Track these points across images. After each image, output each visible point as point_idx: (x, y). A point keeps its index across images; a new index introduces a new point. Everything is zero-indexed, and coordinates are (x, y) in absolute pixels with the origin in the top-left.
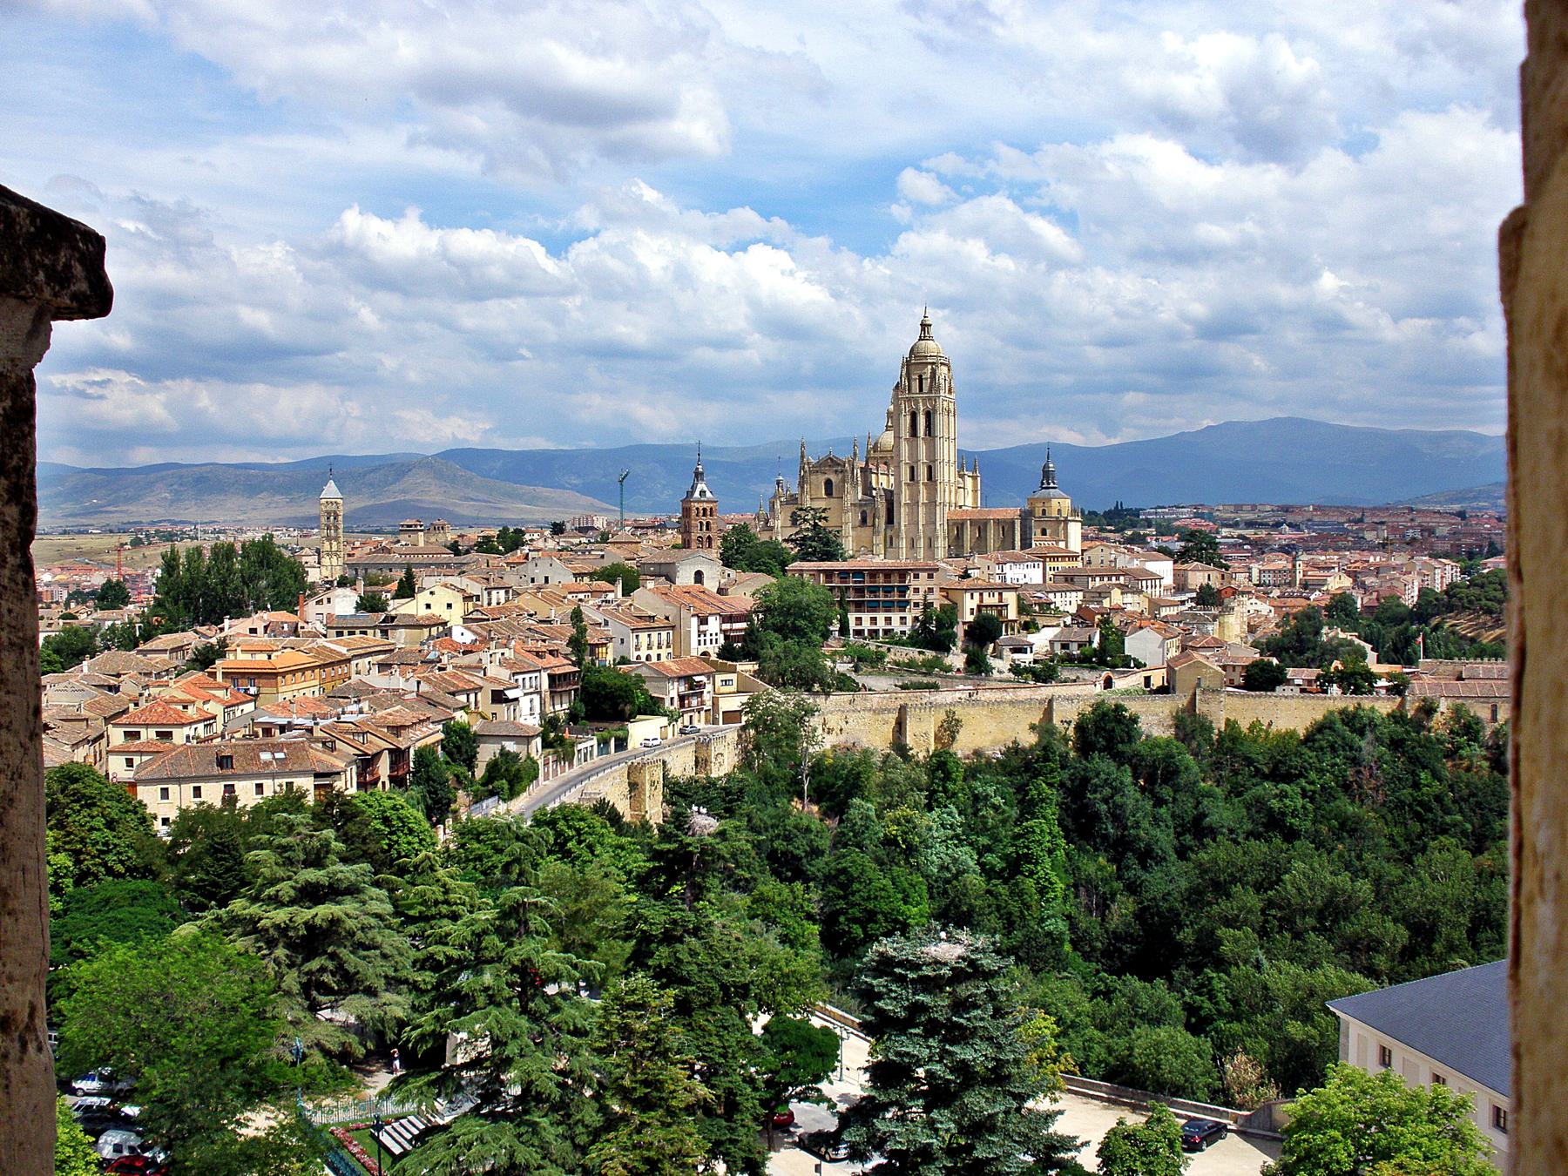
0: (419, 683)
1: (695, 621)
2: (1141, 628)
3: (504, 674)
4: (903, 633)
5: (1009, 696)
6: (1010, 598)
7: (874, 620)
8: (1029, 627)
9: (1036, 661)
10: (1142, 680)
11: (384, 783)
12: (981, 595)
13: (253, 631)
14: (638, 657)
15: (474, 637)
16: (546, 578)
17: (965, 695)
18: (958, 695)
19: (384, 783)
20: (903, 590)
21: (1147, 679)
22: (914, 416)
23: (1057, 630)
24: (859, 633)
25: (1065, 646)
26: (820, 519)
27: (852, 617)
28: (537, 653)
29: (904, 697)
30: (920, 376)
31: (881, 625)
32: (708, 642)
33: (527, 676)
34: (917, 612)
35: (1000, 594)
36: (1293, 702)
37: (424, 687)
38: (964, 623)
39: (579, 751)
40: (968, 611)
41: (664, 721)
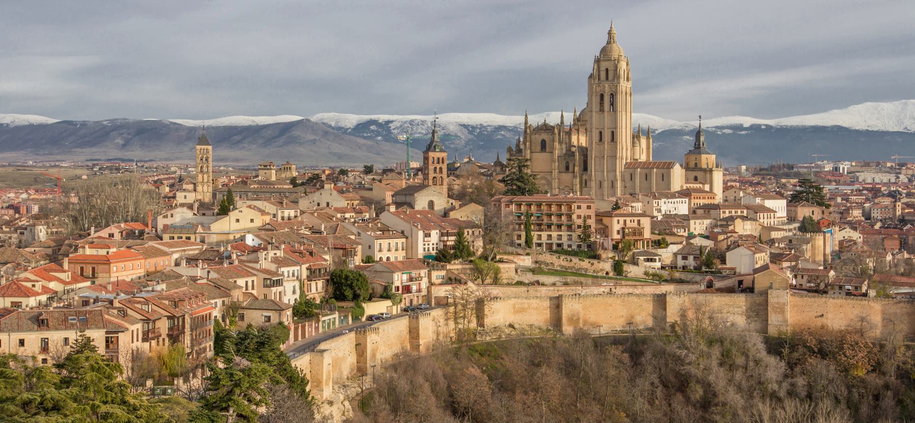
0: (209, 272)
1: (421, 234)
2: (739, 246)
3: (273, 267)
4: (570, 246)
5: (638, 291)
6: (646, 222)
7: (550, 237)
8: (659, 244)
9: (663, 268)
10: (737, 283)
11: (164, 339)
12: (625, 221)
13: (111, 235)
14: (381, 258)
15: (260, 242)
16: (328, 204)
17: (607, 290)
18: (602, 289)
19: (164, 339)
20: (569, 216)
21: (740, 282)
22: (602, 96)
23: (680, 246)
24: (540, 245)
25: (685, 258)
26: (524, 166)
27: (535, 234)
28: (300, 253)
29: (563, 290)
30: (607, 70)
31: (555, 240)
32: (431, 249)
33: (291, 269)
34: (579, 232)
35: (639, 221)
36: (839, 301)
37: (213, 275)
38: (612, 239)
39: (324, 321)
40: (615, 232)
41: (388, 303)
